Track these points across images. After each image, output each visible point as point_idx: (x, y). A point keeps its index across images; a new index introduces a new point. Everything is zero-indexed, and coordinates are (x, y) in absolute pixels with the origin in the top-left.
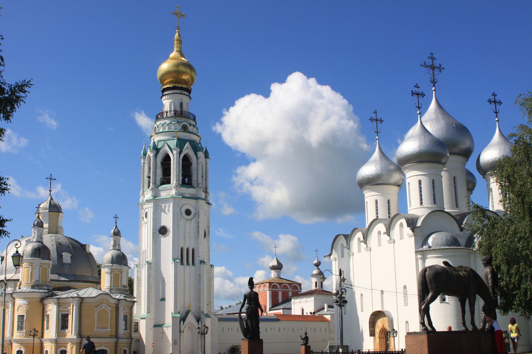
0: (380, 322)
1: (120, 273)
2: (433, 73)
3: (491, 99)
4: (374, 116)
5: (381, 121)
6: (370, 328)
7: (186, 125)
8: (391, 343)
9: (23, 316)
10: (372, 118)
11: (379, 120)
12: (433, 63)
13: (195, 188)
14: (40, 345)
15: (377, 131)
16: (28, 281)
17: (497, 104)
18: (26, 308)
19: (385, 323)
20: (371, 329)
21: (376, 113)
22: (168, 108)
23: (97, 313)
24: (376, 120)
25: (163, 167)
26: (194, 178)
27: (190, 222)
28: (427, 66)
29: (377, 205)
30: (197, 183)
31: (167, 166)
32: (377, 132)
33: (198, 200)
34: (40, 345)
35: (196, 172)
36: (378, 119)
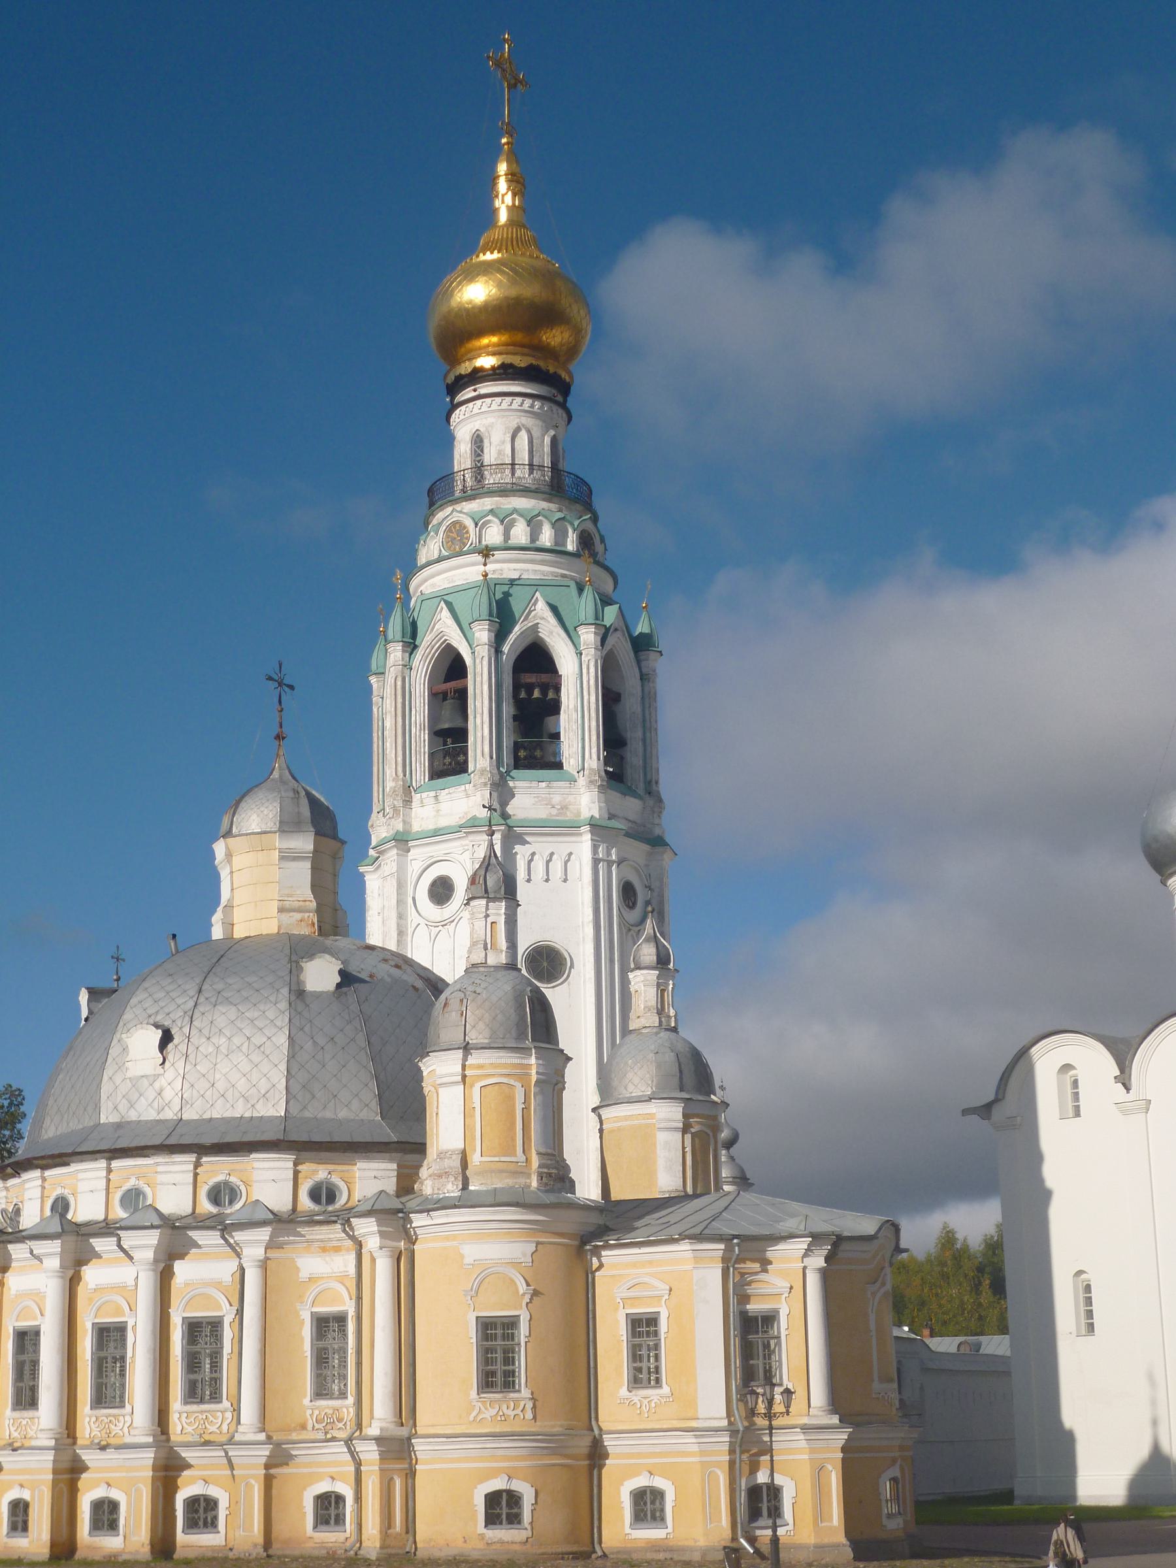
1: (711, 1134)
7: (589, 534)
9: (511, 1324)
13: (640, 797)
14: (587, 1462)
16: (509, 1150)
18: (528, 1285)
22: (500, 453)
23: (874, 1311)
25: (523, 695)
26: (633, 756)
27: (635, 934)
30: (645, 774)
31: (537, 694)
33: (660, 849)
34: (587, 1462)
35: (640, 734)
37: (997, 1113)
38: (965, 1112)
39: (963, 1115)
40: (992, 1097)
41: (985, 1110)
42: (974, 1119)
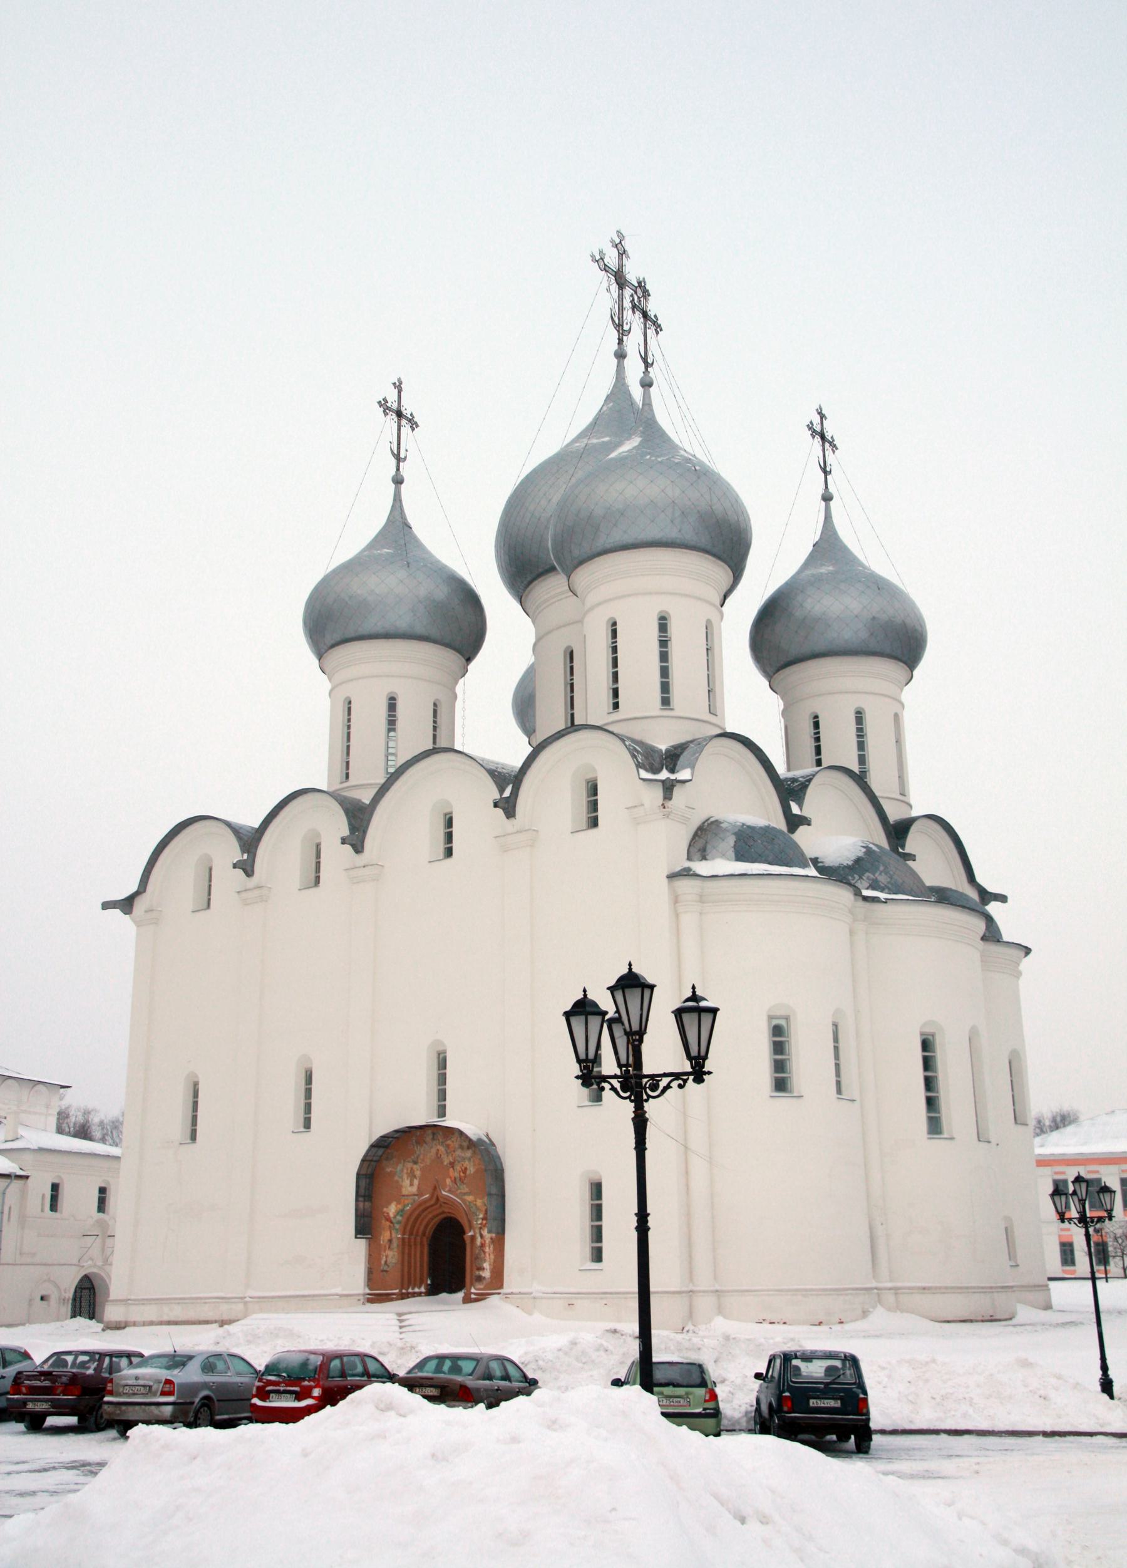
0: (415, 1177)
2: (621, 298)
3: (815, 425)
4: (392, 397)
5: (414, 425)
6: (357, 1200)
8: (482, 1269)
10: (385, 400)
11: (407, 419)
12: (621, 266)
15: (399, 452)
17: (827, 445)
19: (448, 1181)
20: (361, 1205)
21: (400, 392)
24: (399, 414)
28: (606, 269)
29: (394, 716)
32: (398, 459)
36: (404, 412)
37: (140, 905)
38: (106, 906)
39: (103, 909)
40: (133, 888)
41: (127, 905)
42: (117, 911)
